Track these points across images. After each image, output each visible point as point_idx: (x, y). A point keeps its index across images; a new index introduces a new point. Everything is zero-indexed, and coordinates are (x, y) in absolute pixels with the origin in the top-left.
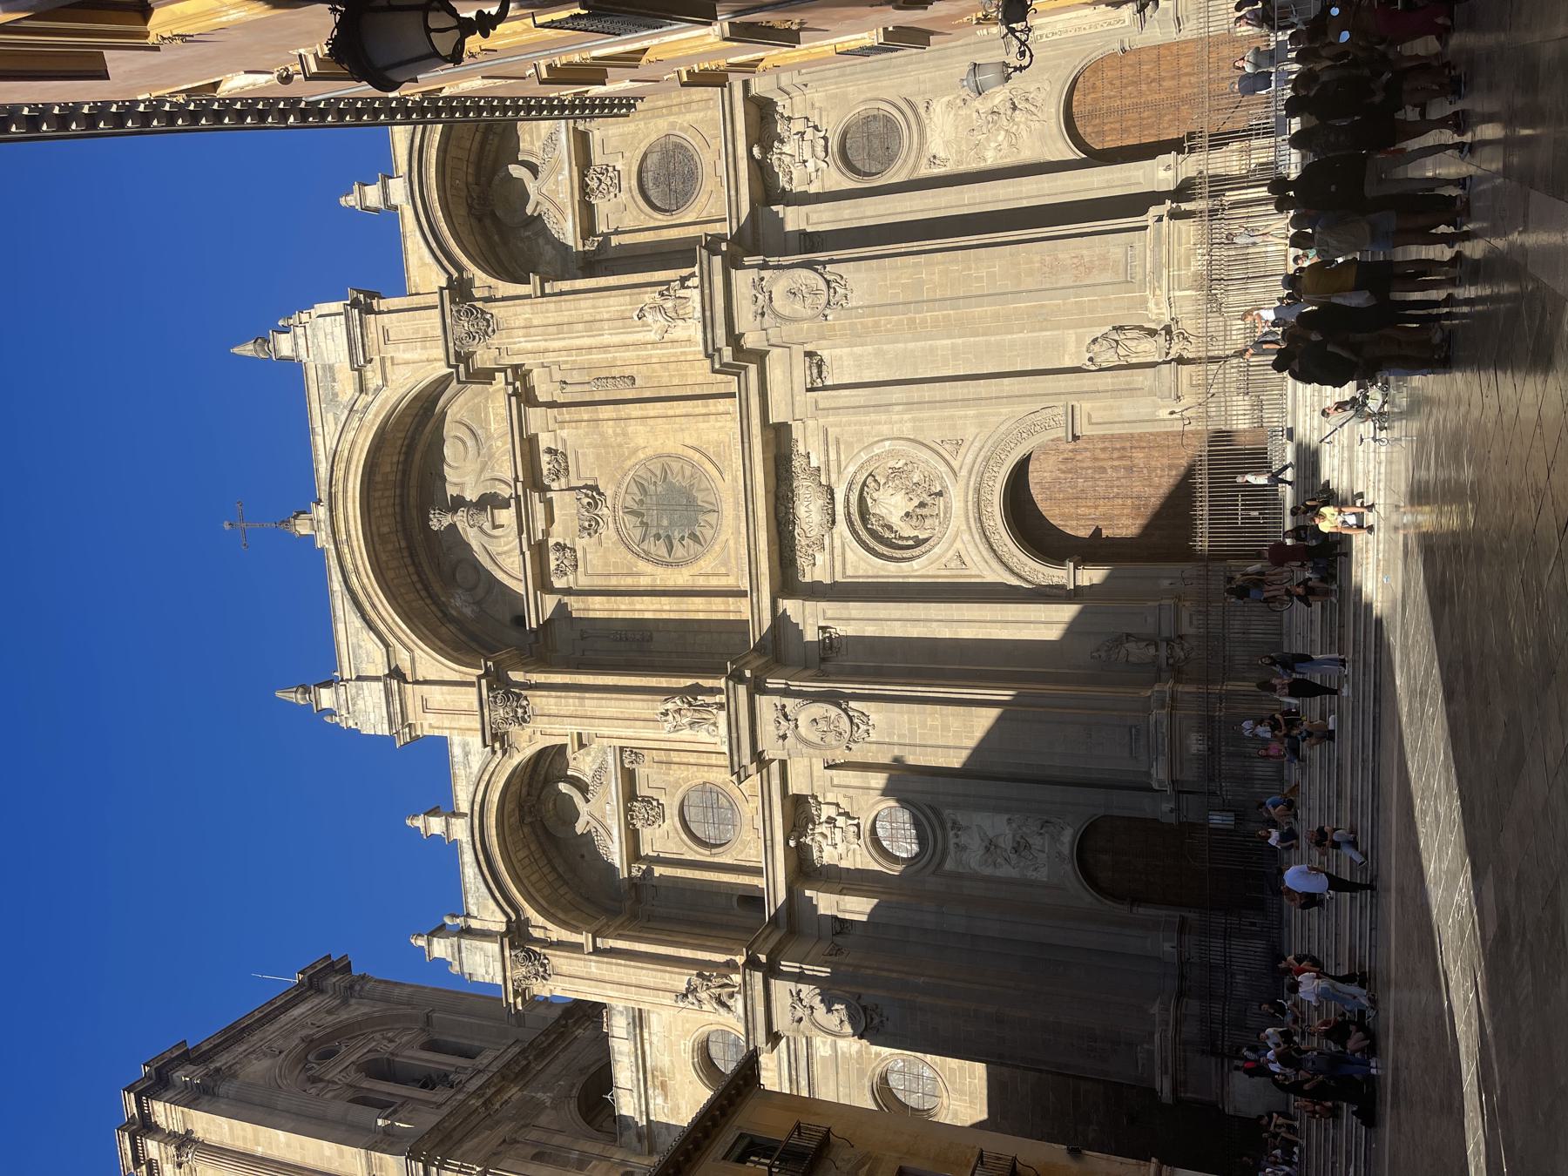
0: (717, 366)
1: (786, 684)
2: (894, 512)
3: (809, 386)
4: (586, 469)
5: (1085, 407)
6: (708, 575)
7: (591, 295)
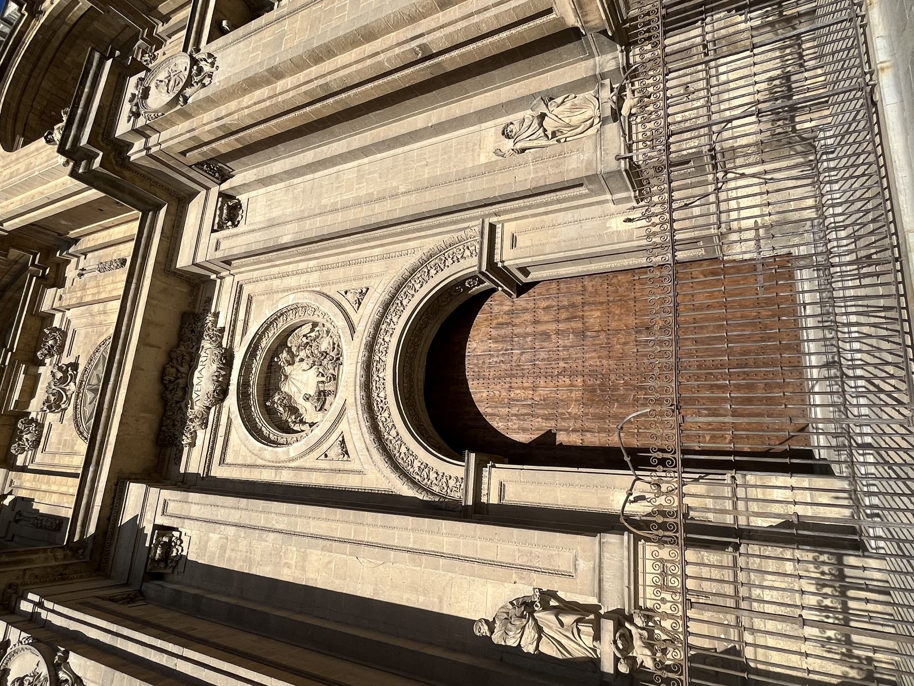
2: (302, 389)
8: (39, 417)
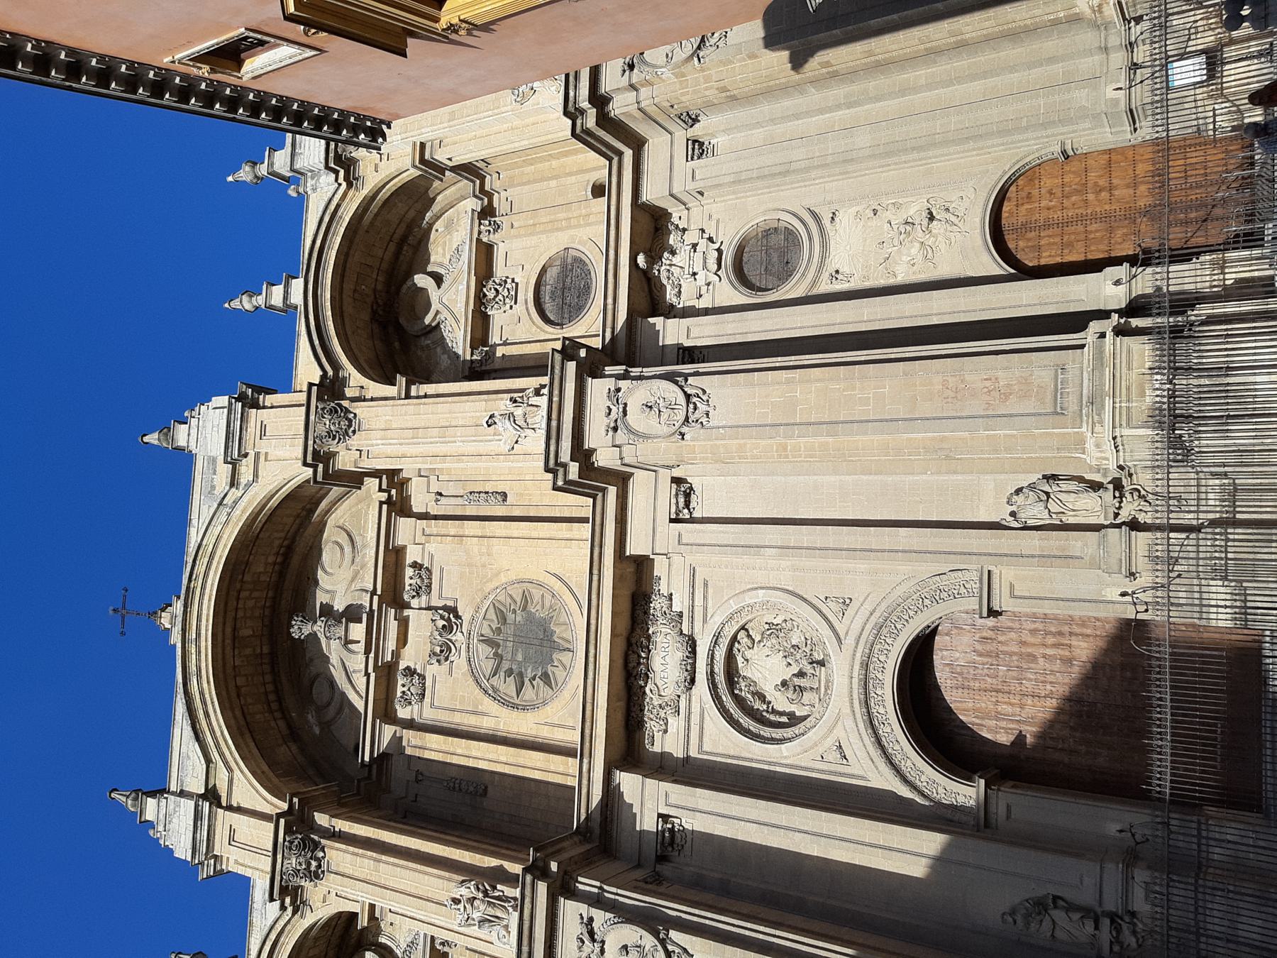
0: (560, 483)
1: (600, 888)
3: (673, 516)
4: (448, 589)
5: (1005, 575)
6: (554, 725)
7: (450, 399)
8: (417, 667)
